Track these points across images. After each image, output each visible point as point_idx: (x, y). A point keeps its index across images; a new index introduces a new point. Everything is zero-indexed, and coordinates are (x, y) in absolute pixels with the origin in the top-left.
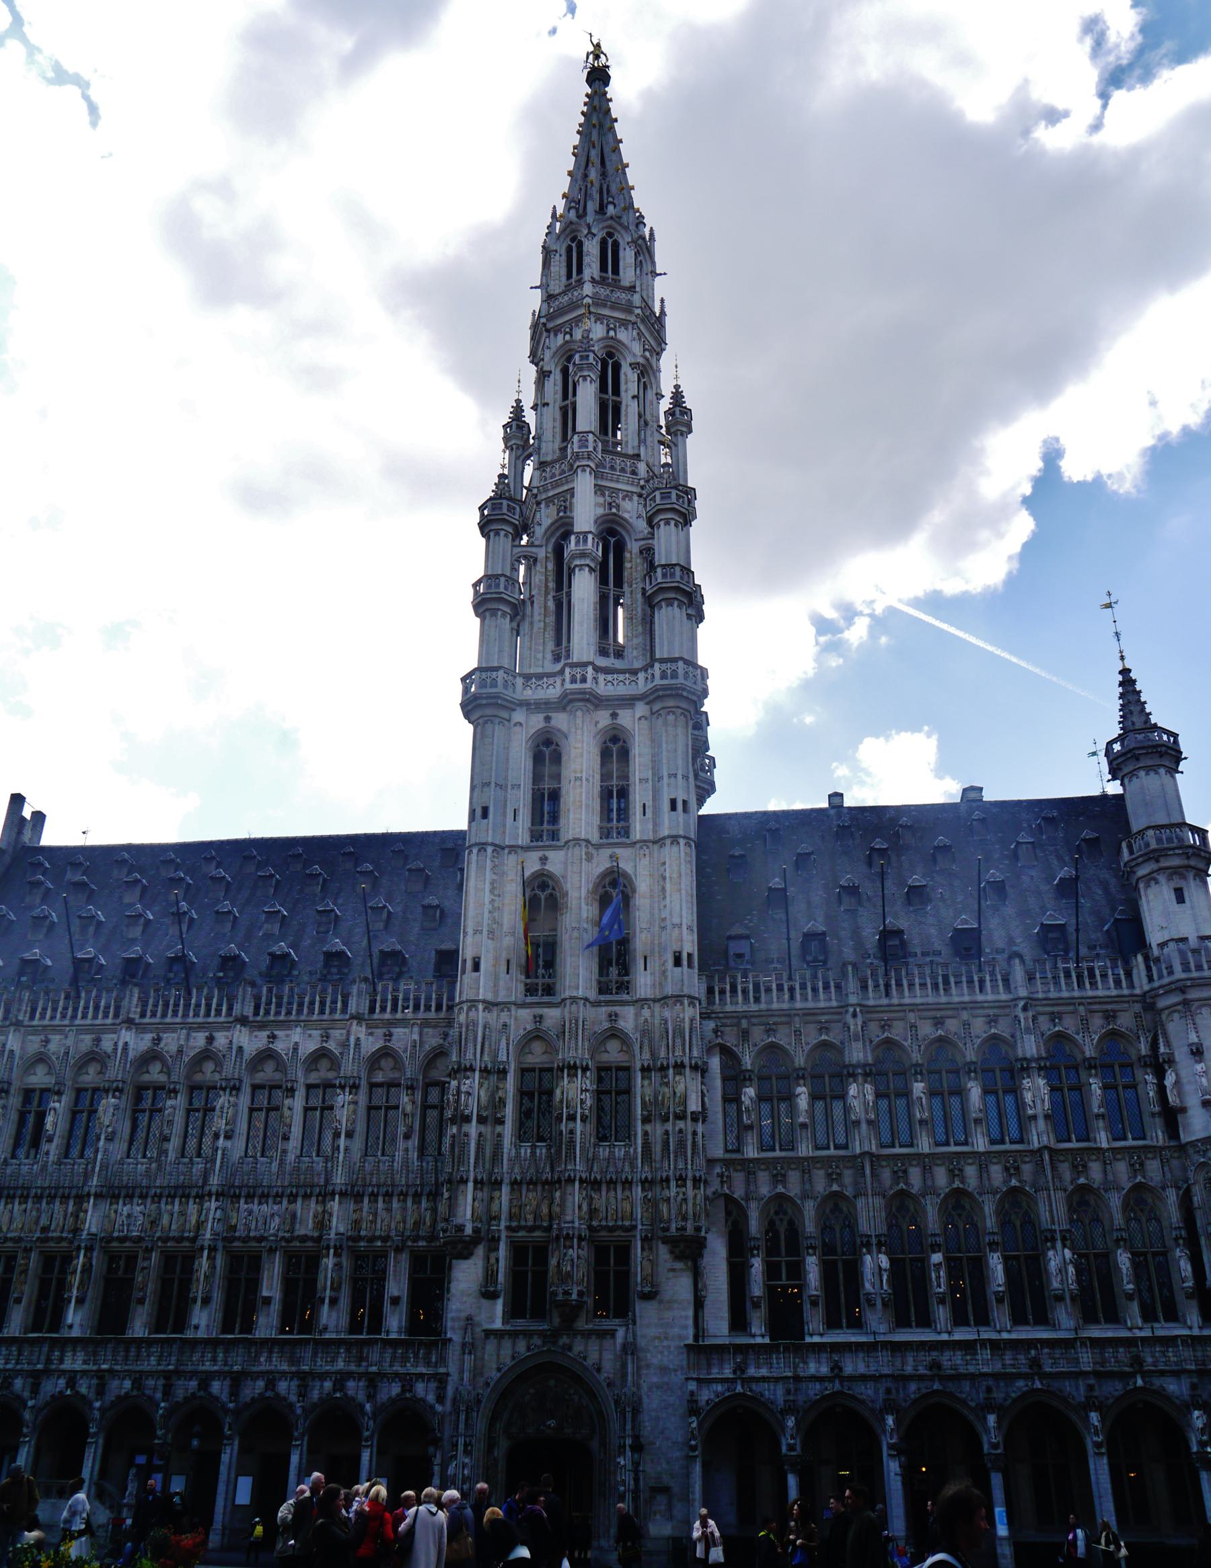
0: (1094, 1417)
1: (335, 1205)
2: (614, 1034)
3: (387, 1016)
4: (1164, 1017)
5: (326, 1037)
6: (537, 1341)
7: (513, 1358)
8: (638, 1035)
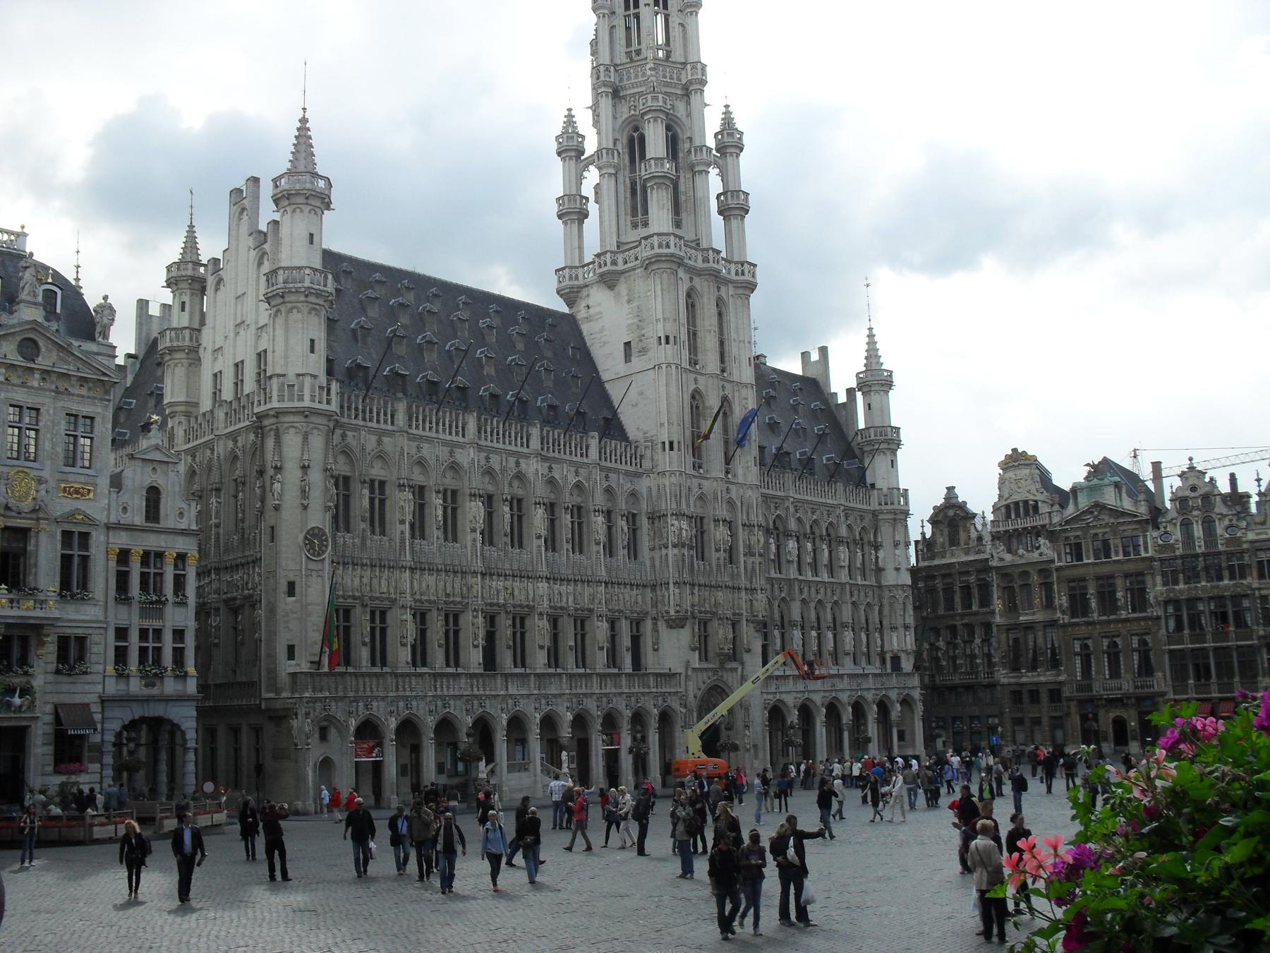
0: (875, 707)
1: (602, 588)
2: (730, 502)
3: (609, 465)
4: (881, 523)
5: (577, 473)
6: (710, 674)
8: (739, 504)
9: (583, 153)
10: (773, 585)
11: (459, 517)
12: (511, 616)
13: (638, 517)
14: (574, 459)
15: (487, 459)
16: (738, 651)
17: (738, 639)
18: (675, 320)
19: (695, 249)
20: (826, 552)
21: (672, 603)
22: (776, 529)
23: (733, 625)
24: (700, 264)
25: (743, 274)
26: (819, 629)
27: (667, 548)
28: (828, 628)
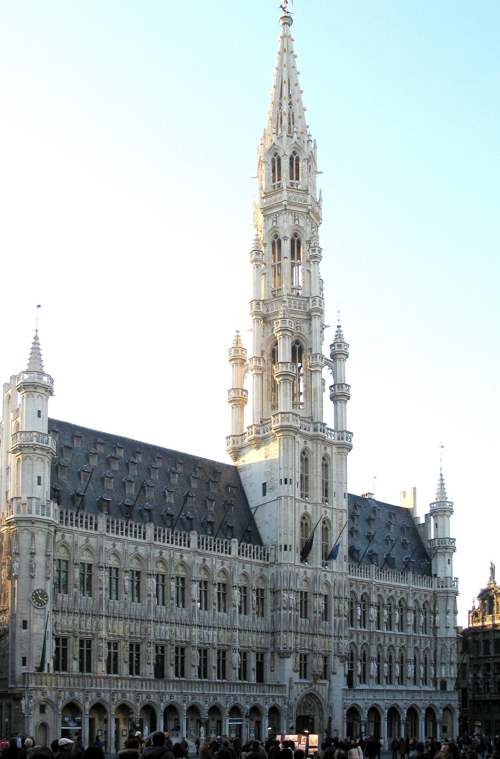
1: (237, 633)
2: (327, 584)
3: (245, 559)
5: (223, 563)
6: (307, 686)
7: (302, 691)
8: (332, 585)
9: (245, 361)
10: (358, 635)
11: (141, 587)
12: (174, 647)
13: (265, 591)
14: (221, 554)
15: (161, 553)
16: (328, 673)
17: (328, 667)
18: (292, 468)
19: (309, 423)
20: (398, 615)
21: (282, 644)
22: (364, 601)
23: (325, 659)
24: (311, 433)
25: (343, 439)
26: (391, 662)
27: (280, 610)
28: (396, 662)
